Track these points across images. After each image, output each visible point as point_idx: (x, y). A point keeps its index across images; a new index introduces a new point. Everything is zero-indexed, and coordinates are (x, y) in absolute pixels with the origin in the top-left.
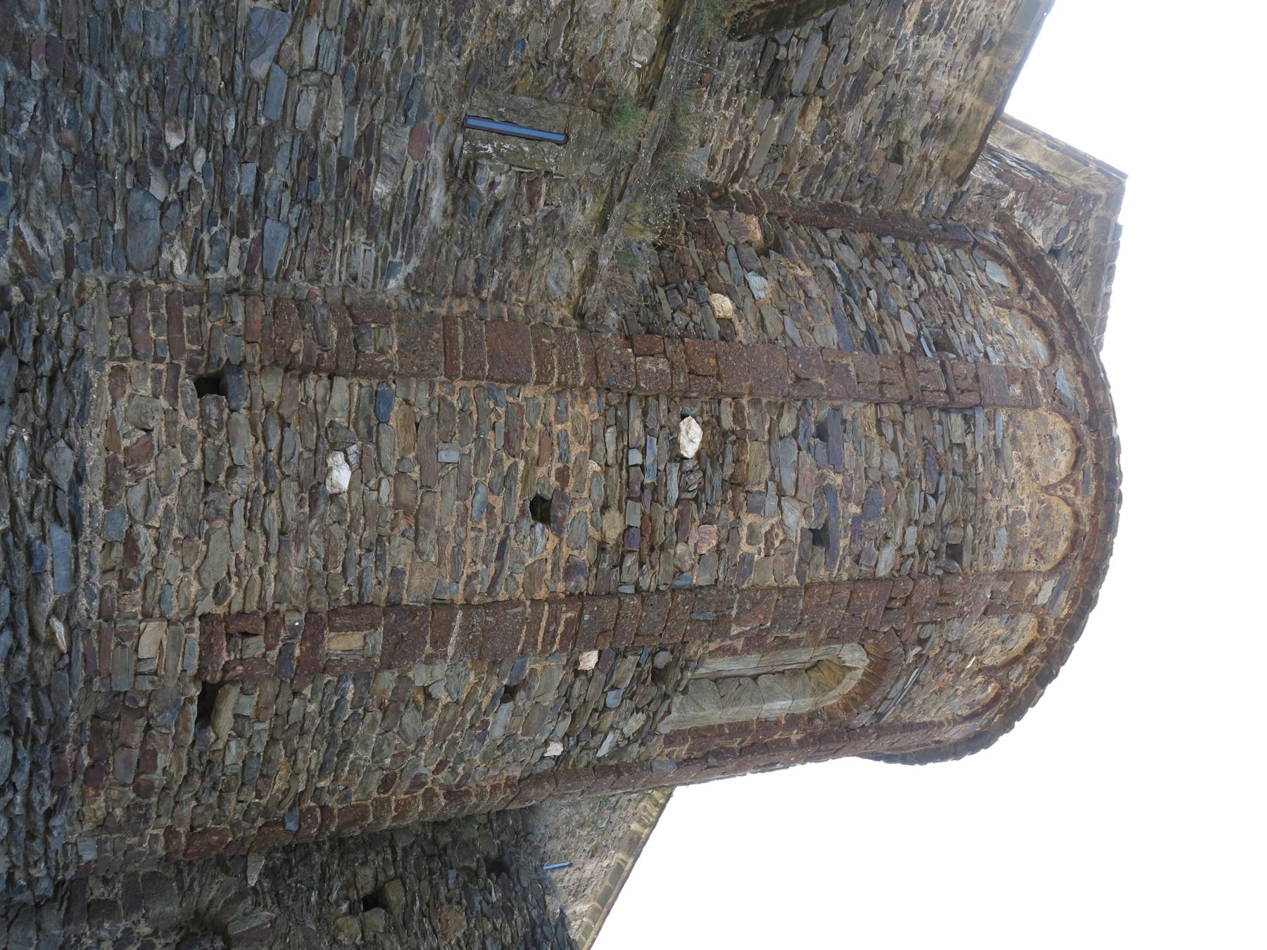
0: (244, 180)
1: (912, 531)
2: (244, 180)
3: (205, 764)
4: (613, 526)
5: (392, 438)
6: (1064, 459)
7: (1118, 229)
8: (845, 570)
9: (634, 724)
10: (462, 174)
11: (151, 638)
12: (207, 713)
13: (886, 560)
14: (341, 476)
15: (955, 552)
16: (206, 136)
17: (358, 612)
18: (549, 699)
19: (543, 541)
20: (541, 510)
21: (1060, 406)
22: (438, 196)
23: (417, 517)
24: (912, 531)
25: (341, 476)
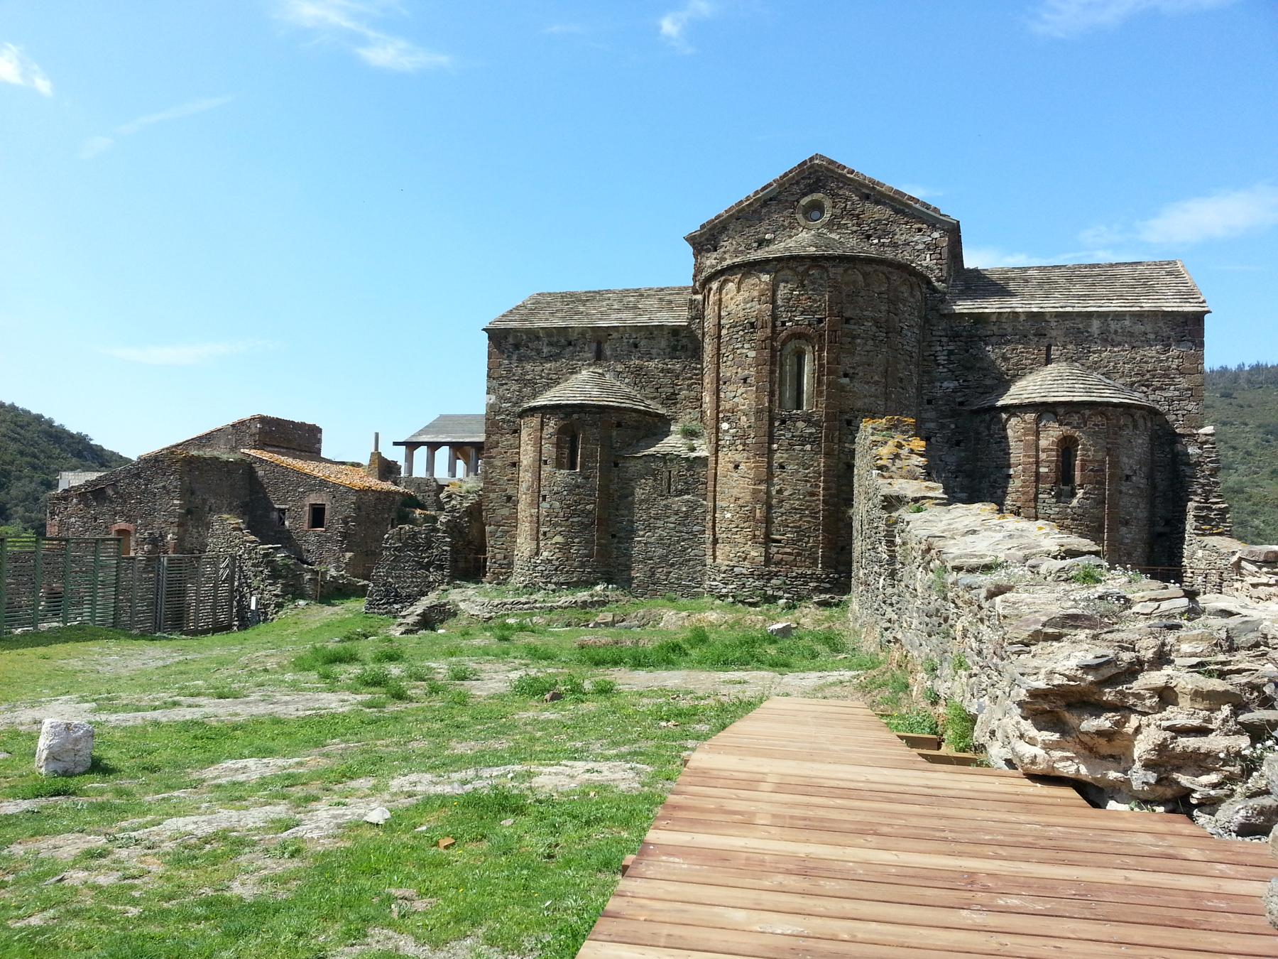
0: (686, 536)
1: (746, 346)
2: (686, 536)
3: (794, 542)
4: (740, 447)
5: (724, 504)
6: (731, 286)
7: (703, 227)
8: (753, 371)
9: (800, 424)
10: (680, 493)
11: (754, 554)
12: (779, 541)
13: (752, 354)
14: (729, 515)
15: (752, 324)
16: (678, 542)
17: (753, 511)
18: (785, 456)
19: (742, 466)
20: (737, 467)
21: (720, 289)
22: (686, 497)
23: (737, 499)
24: (746, 346)
25: (729, 515)
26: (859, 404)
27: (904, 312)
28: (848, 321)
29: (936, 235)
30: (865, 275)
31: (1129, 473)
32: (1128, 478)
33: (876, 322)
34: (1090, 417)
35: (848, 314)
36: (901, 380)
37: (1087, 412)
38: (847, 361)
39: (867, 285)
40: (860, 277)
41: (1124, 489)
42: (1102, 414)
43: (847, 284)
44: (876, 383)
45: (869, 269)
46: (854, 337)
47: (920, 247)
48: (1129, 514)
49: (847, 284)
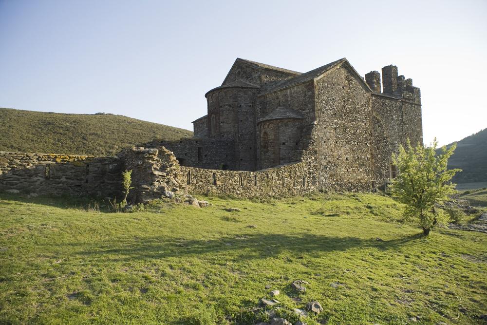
26: (225, 130)
27: (240, 101)
28: (221, 106)
29: (259, 73)
30: (225, 93)
31: (283, 142)
32: (284, 144)
33: (229, 105)
34: (269, 125)
35: (221, 105)
36: (241, 121)
37: (268, 124)
38: (221, 118)
39: (226, 95)
40: (224, 94)
41: (281, 147)
42: (272, 123)
43: (220, 96)
44: (230, 123)
45: (225, 91)
46: (223, 111)
47: (257, 78)
48: (284, 156)
49: (220, 96)
